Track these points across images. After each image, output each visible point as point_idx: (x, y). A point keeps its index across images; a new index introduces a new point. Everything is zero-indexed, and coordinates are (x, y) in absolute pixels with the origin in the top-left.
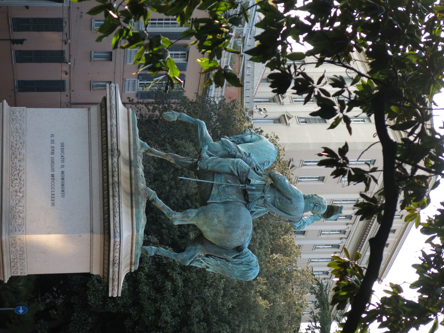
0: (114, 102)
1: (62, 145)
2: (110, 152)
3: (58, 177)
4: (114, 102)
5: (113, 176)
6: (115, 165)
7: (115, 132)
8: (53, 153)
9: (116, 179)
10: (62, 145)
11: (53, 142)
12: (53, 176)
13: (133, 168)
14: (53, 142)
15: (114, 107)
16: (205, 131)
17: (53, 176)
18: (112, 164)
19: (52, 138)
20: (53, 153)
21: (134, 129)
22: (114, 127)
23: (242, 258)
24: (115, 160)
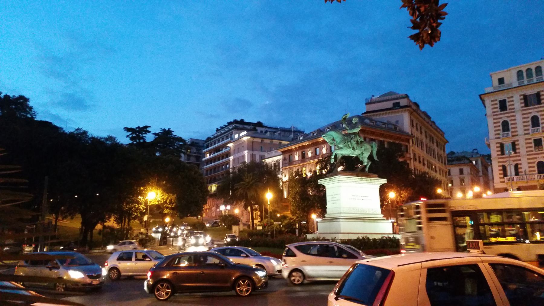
1: (353, 196)
3: (362, 198)
8: (355, 199)
10: (353, 196)
11: (352, 199)
14: (352, 199)
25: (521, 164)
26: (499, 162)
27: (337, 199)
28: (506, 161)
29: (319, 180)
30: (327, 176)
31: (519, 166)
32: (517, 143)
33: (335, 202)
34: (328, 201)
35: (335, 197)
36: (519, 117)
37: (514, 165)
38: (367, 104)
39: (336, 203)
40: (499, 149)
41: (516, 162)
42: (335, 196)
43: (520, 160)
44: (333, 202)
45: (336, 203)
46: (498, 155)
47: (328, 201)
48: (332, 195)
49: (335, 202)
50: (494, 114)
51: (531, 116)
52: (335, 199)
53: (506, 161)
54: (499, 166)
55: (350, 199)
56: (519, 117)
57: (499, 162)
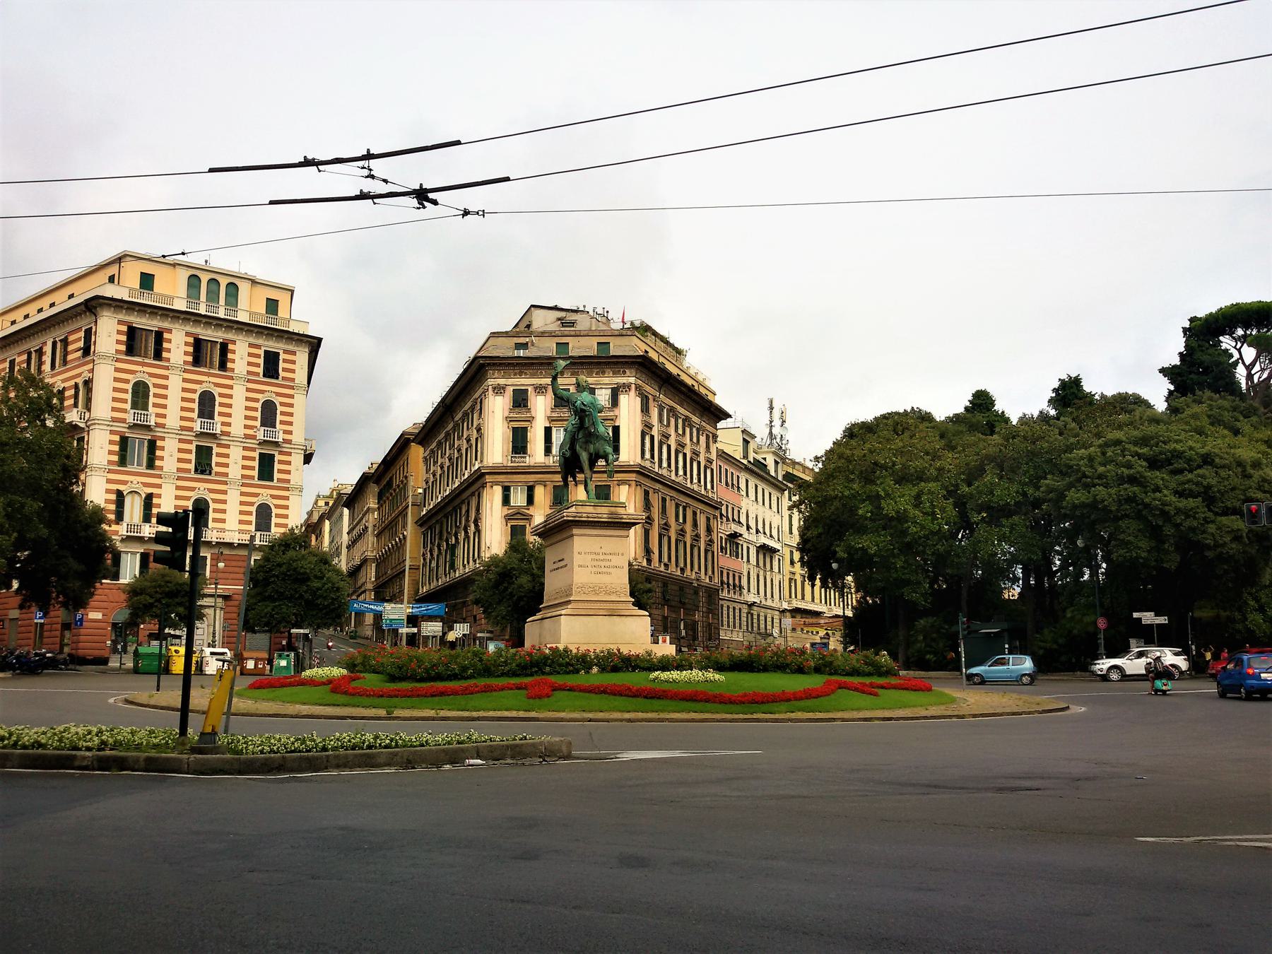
25: (159, 496)
26: (109, 481)
28: (125, 483)
31: (155, 501)
32: (159, 443)
33: (609, 570)
36: (175, 383)
37: (144, 496)
39: (610, 573)
40: (116, 448)
41: (150, 490)
43: (159, 486)
44: (600, 570)
45: (610, 573)
46: (110, 462)
49: (609, 570)
50: (250, 378)
51: (200, 389)
52: (607, 564)
53: (125, 483)
54: (108, 491)
56: (175, 383)
57: (109, 481)
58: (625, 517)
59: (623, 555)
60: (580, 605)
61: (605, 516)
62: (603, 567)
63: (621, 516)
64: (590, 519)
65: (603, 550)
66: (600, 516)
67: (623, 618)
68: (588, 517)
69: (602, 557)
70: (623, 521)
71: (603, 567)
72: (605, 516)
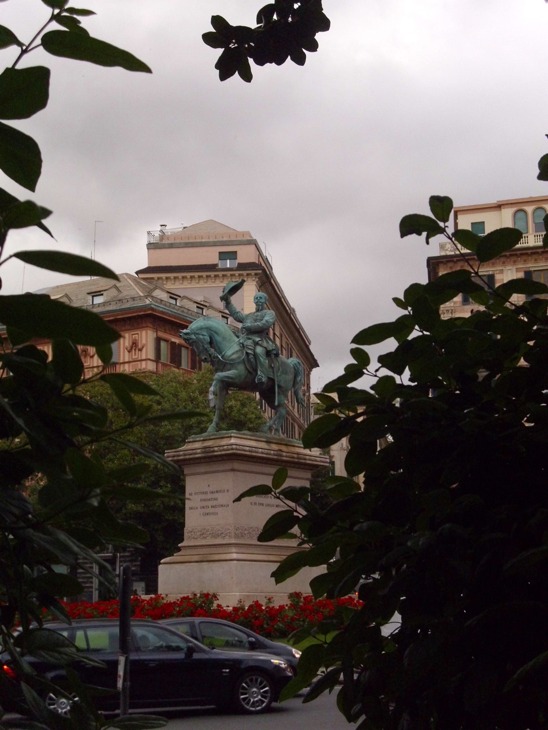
0: (248, 448)
2: (279, 458)
4: (248, 448)
5: (293, 458)
6: (288, 454)
7: (266, 451)
8: (263, 505)
9: (296, 456)
11: (255, 504)
12: (277, 506)
13: (271, 441)
15: (251, 449)
16: (229, 375)
17: (277, 506)
18: (286, 456)
19: (253, 503)
20: (263, 505)
21: (244, 434)
22: (263, 451)
23: (298, 368)
24: (284, 454)
27: (221, 504)
29: (166, 451)
30: (189, 440)
34: (191, 508)
35: (216, 499)
38: (151, 246)
39: (217, 514)
42: (216, 495)
45: (217, 514)
47: (191, 508)
48: (206, 493)
55: (251, 503)
58: (216, 449)
59: (228, 491)
60: (189, 552)
61: (199, 451)
62: (210, 507)
63: (212, 449)
64: (188, 457)
65: (211, 489)
66: (194, 451)
67: (211, 564)
68: (185, 455)
69: (209, 496)
70: (216, 453)
71: (210, 507)
72: (199, 451)
